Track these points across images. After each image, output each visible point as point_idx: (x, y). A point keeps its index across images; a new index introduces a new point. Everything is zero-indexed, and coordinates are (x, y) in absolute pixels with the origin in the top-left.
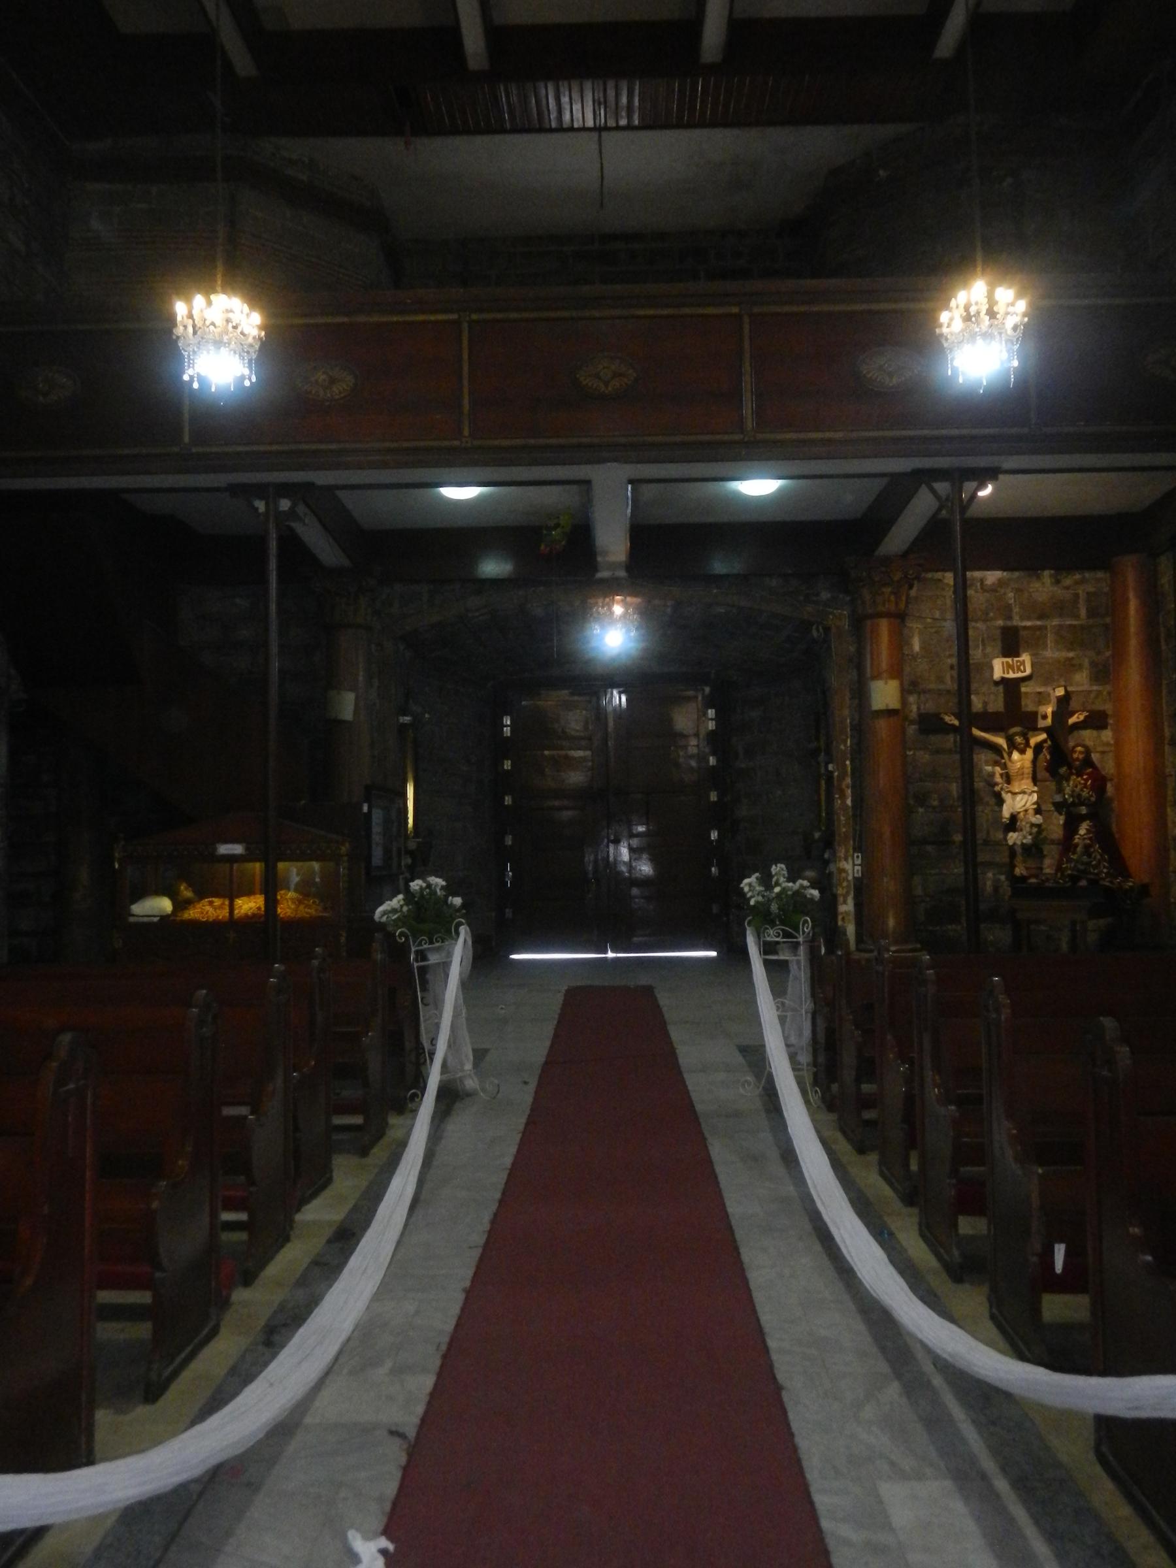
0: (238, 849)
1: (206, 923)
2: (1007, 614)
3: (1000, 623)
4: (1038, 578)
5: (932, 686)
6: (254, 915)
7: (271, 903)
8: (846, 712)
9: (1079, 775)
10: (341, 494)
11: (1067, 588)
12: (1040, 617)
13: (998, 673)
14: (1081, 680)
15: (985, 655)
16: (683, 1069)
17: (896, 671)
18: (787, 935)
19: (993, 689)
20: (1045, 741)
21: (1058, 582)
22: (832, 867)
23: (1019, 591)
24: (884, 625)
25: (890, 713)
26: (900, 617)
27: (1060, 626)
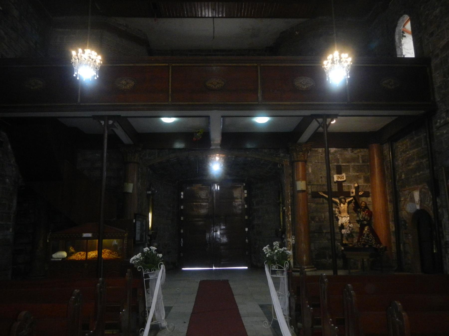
0: (90, 235)
1: (78, 260)
3: (336, 164)
4: (347, 150)
5: (315, 183)
6: (94, 258)
7: (100, 254)
8: (289, 191)
9: (364, 211)
10: (129, 119)
11: (356, 154)
13: (335, 179)
14: (361, 182)
16: (241, 316)
17: (304, 179)
18: (280, 268)
19: (335, 184)
20: (352, 200)
21: (352, 152)
22: (285, 240)
23: (341, 154)
24: (300, 164)
25: (303, 191)
26: (305, 162)
27: (354, 165)
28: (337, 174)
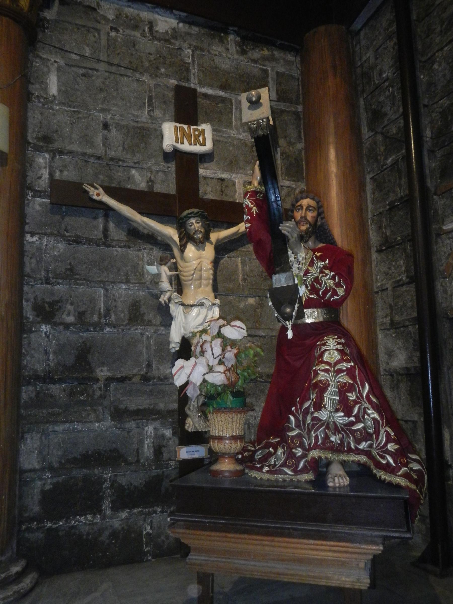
3: (173, 82)
4: (222, 41)
5: (75, 148)
11: (255, 61)
12: (223, 87)
15: (153, 119)
28: (178, 119)
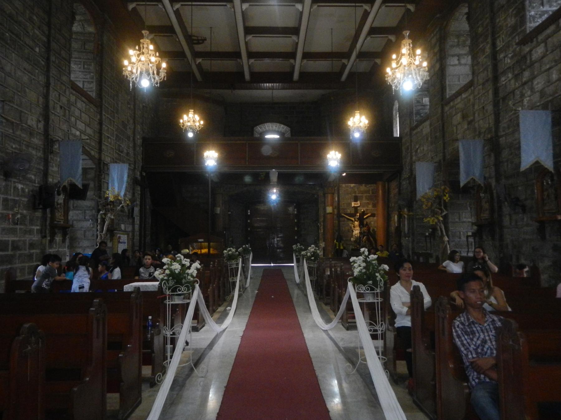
0: (202, 240)
2: (355, 192)
7: (209, 250)
13: (353, 205)
14: (370, 207)
17: (332, 205)
23: (358, 188)
25: (330, 213)
